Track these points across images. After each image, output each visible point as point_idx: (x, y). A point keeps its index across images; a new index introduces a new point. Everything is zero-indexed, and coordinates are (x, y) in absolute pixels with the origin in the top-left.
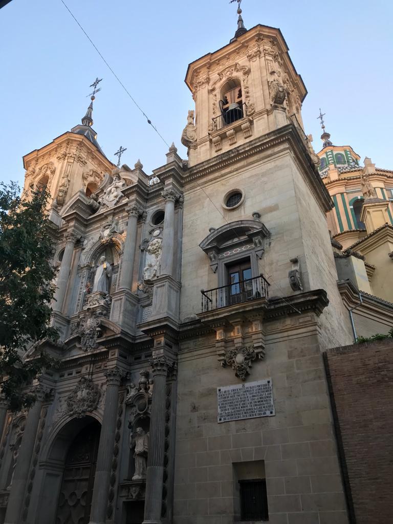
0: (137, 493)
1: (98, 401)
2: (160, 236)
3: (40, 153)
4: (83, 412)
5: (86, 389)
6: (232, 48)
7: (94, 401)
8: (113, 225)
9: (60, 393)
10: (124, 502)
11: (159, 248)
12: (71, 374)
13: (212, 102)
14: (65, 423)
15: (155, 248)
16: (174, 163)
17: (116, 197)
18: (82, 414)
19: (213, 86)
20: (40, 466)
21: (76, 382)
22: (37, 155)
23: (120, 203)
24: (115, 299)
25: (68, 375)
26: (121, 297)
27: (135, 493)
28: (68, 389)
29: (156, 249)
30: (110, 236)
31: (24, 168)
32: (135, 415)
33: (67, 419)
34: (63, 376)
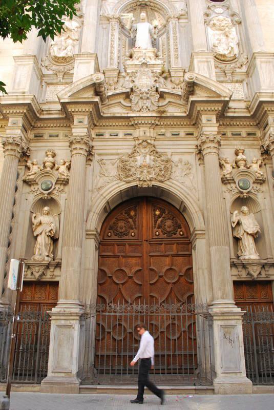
4: (150, 180)
5: (150, 155)
9: (100, 155)
11: (227, 26)
15: (223, 25)
18: (149, 182)
20: (87, 235)
21: (131, 145)
24: (199, 59)
25: (111, 135)
26: (209, 60)
28: (115, 151)
29: (223, 26)
32: (233, 193)
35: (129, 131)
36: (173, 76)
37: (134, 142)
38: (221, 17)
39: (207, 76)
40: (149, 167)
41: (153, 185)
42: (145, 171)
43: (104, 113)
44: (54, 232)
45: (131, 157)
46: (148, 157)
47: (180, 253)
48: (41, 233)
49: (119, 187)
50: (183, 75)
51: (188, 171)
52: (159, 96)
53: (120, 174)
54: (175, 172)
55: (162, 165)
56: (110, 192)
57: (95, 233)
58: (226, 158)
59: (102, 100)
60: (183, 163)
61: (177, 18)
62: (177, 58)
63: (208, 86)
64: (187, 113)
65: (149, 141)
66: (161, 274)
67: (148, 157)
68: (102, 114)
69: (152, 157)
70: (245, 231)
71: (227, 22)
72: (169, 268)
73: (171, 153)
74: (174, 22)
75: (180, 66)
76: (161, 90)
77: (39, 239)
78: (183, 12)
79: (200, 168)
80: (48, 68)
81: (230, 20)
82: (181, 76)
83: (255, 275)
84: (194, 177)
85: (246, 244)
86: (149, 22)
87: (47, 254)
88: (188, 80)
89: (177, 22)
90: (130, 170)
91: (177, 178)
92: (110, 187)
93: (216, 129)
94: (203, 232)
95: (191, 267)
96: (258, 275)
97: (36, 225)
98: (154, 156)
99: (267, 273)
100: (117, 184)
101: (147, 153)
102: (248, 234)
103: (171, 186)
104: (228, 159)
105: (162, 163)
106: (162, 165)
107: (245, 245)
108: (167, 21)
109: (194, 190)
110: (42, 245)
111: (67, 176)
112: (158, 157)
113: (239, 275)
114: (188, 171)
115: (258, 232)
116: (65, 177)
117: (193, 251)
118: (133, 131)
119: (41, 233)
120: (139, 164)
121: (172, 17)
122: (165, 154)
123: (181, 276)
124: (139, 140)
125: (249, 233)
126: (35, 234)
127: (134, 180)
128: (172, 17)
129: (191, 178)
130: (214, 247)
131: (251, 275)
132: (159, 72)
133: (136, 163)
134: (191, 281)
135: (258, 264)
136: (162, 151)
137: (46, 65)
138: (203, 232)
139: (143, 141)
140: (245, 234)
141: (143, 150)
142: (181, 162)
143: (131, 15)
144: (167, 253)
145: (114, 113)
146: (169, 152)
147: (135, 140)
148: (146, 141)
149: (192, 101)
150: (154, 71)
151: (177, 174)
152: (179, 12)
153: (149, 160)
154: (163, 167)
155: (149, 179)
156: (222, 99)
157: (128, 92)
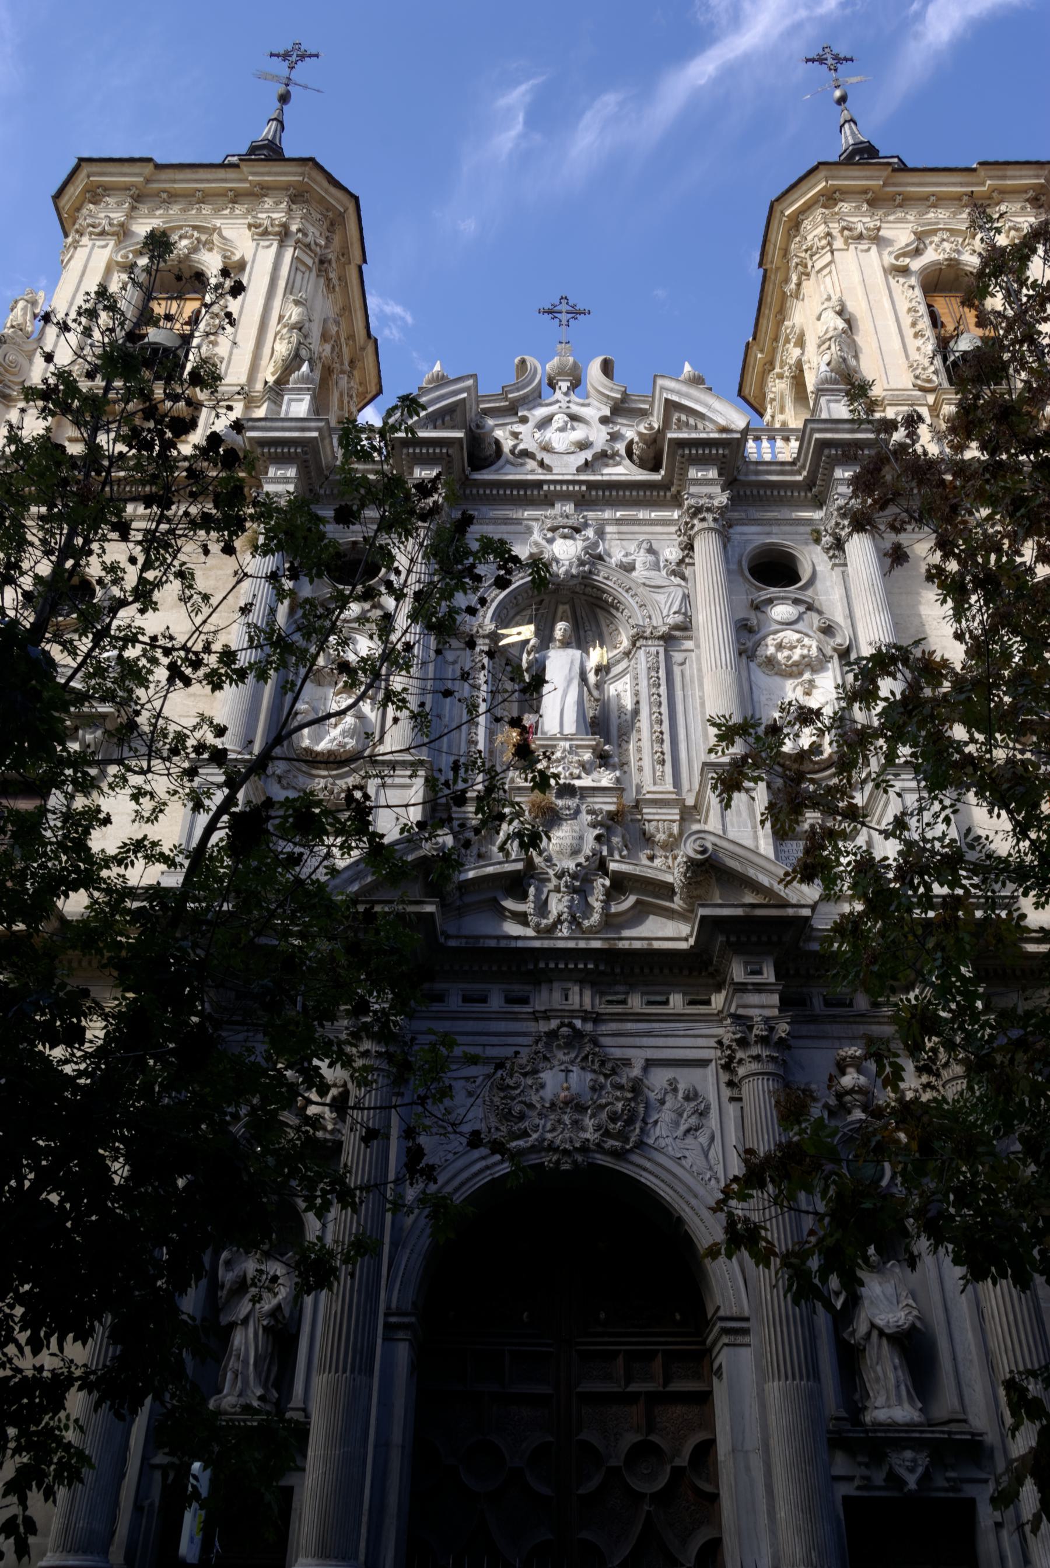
0: (920, 1470)
1: (644, 1121)
2: (799, 626)
3: (167, 182)
5: (583, 1068)
6: (954, 184)
7: (630, 1121)
8: (590, 533)
10: (846, 1499)
12: (484, 1000)
13: (903, 306)
14: (486, 1178)
16: (809, 426)
17: (583, 445)
19: (907, 260)
22: (148, 181)
23: (594, 473)
25: (466, 999)
27: (911, 1470)
29: (796, 664)
30: (582, 563)
31: (57, 196)
33: (495, 1164)
34: (440, 998)
35: (517, 989)
36: (649, 821)
37: (533, 1024)
38: (789, 636)
39: (748, 843)
40: (581, 1108)
41: (590, 1164)
42: (566, 1119)
43: (448, 937)
44: (287, 1315)
45: (525, 1075)
46: (574, 1077)
47: (676, 1386)
48: (245, 1321)
49: (487, 1168)
50: (677, 817)
51: (693, 1121)
52: (607, 883)
53: (493, 1125)
54: (656, 1122)
55: (617, 1099)
56: (463, 1184)
57: (413, 1319)
58: (808, 1084)
59: (443, 906)
60: (680, 1095)
61: (660, 638)
62: (663, 762)
63: (752, 873)
64: (692, 941)
65: (578, 1023)
66: (613, 1462)
67: (576, 1073)
68: (442, 940)
69: (590, 1076)
70: (873, 1326)
71: (805, 652)
72: (639, 1438)
73: (642, 1062)
74: (653, 650)
75: (671, 789)
76: (613, 866)
77: (238, 1339)
78: (679, 618)
79: (731, 1109)
80: (284, 782)
81: (814, 644)
82: (674, 821)
83: (912, 1481)
84: (712, 1139)
85: (879, 1368)
86: (579, 647)
87: (259, 1392)
88: (692, 854)
89: (661, 650)
90: (522, 1117)
91: (662, 1143)
92: (462, 1170)
93: (775, 999)
94: (744, 1325)
95: (709, 1436)
96: (919, 1482)
97: (230, 1290)
98: (594, 1071)
99: (952, 1474)
100: (483, 1158)
101: (572, 1062)
102: (882, 1333)
103: (645, 1169)
104: (814, 1087)
105: (618, 1093)
106: (617, 1099)
107: (875, 1372)
108: (634, 644)
109: (713, 1181)
110: (246, 1362)
111: (332, 1132)
112: (606, 1076)
113: (863, 1478)
114: (693, 1121)
115: (913, 1326)
116: (328, 1137)
117: (715, 1380)
118: (527, 988)
119: (245, 1321)
120: (548, 1093)
121: (647, 634)
122: (627, 1063)
123: (678, 1472)
124: (548, 1018)
125: (887, 1331)
126: (224, 1320)
127: (533, 1146)
128: (647, 634)
129: (703, 1140)
130: (776, 1383)
131: (902, 1483)
132: (609, 812)
133: (542, 1093)
134: (708, 1488)
135: (917, 1445)
136: (618, 1053)
137: (278, 772)
138: (744, 1325)
139: (562, 1025)
140: (875, 1334)
141: (560, 1055)
142: (675, 1090)
143: (527, 631)
144: (633, 1388)
145: (478, 938)
146: (638, 1058)
147: (536, 1020)
148: (570, 1025)
149: (703, 917)
150: (597, 807)
151: (661, 1130)
152: (670, 621)
153: (579, 1080)
154: (620, 1105)
155: (578, 1145)
156: (790, 912)
157: (519, 871)
